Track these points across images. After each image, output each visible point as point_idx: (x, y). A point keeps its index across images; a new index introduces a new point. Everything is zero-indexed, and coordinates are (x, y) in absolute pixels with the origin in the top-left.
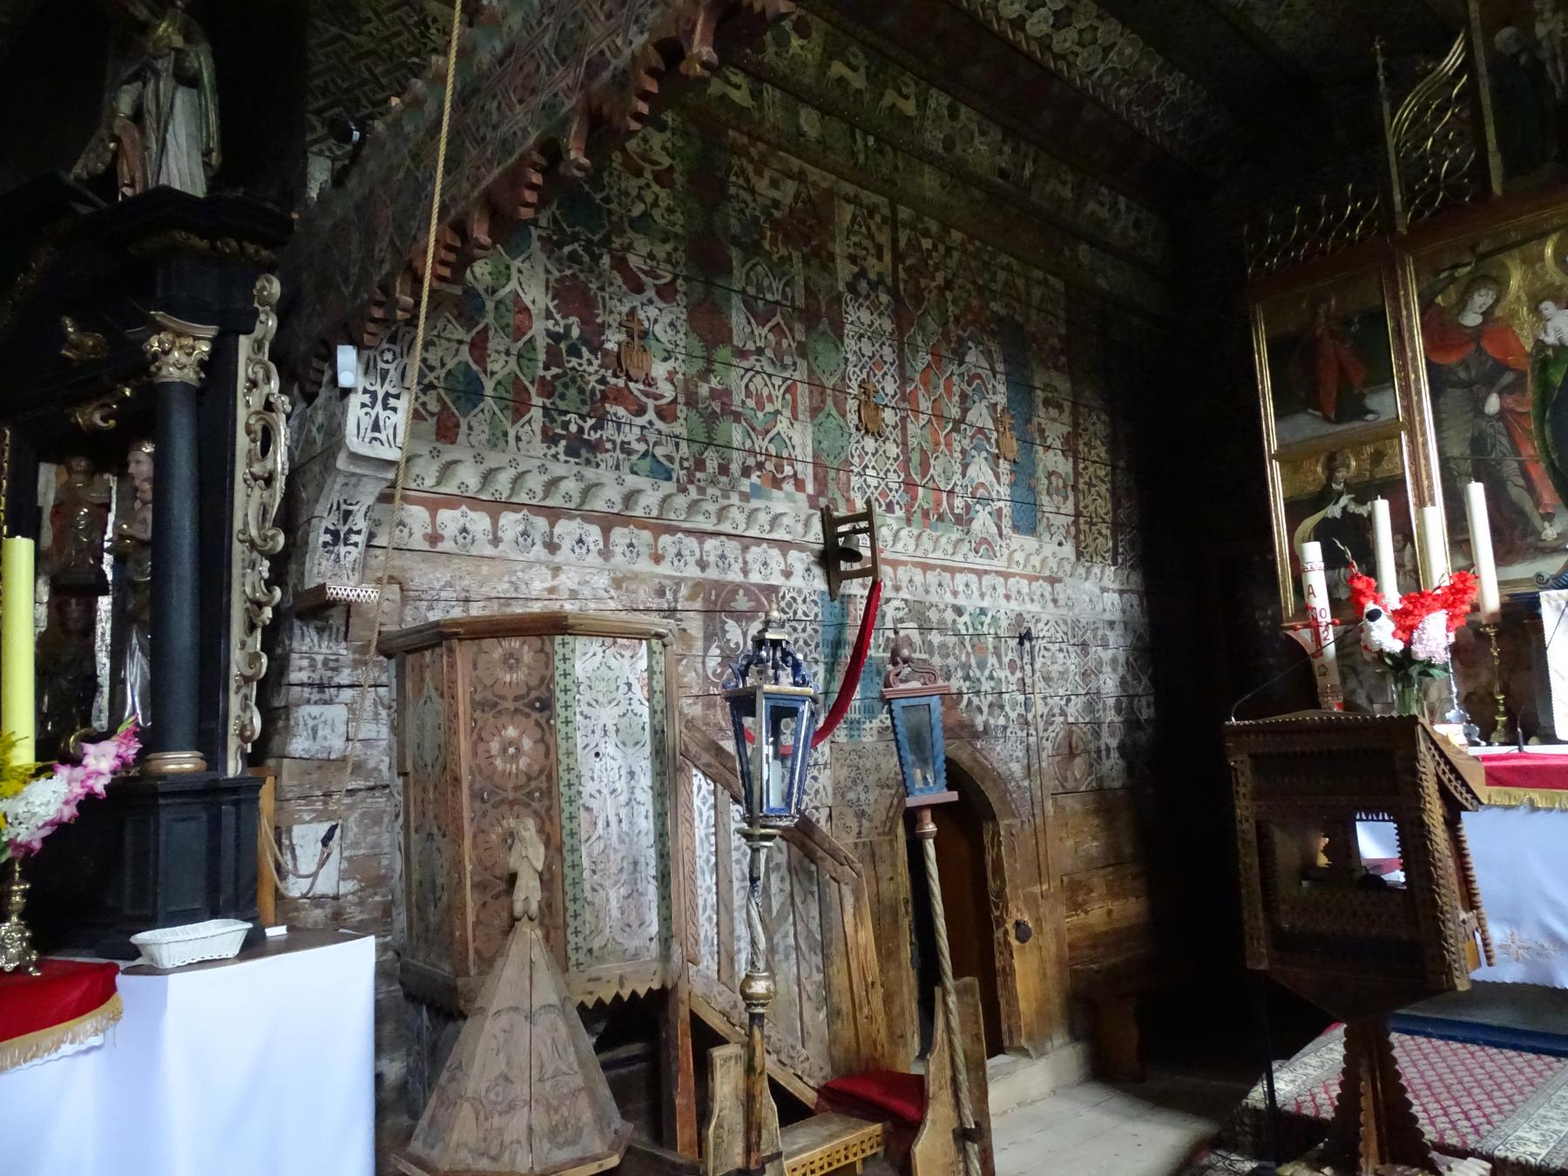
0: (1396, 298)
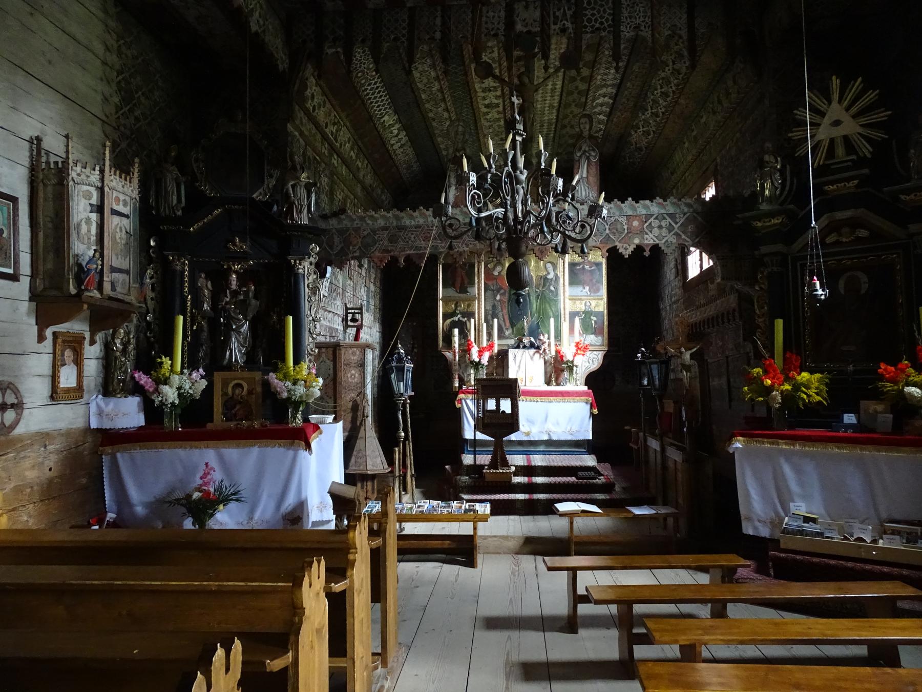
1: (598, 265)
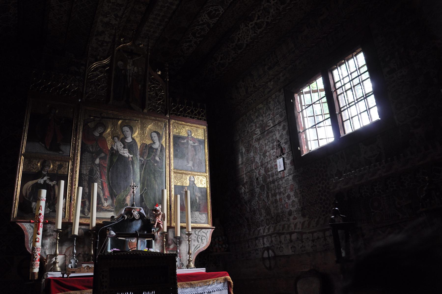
1: (200, 142)
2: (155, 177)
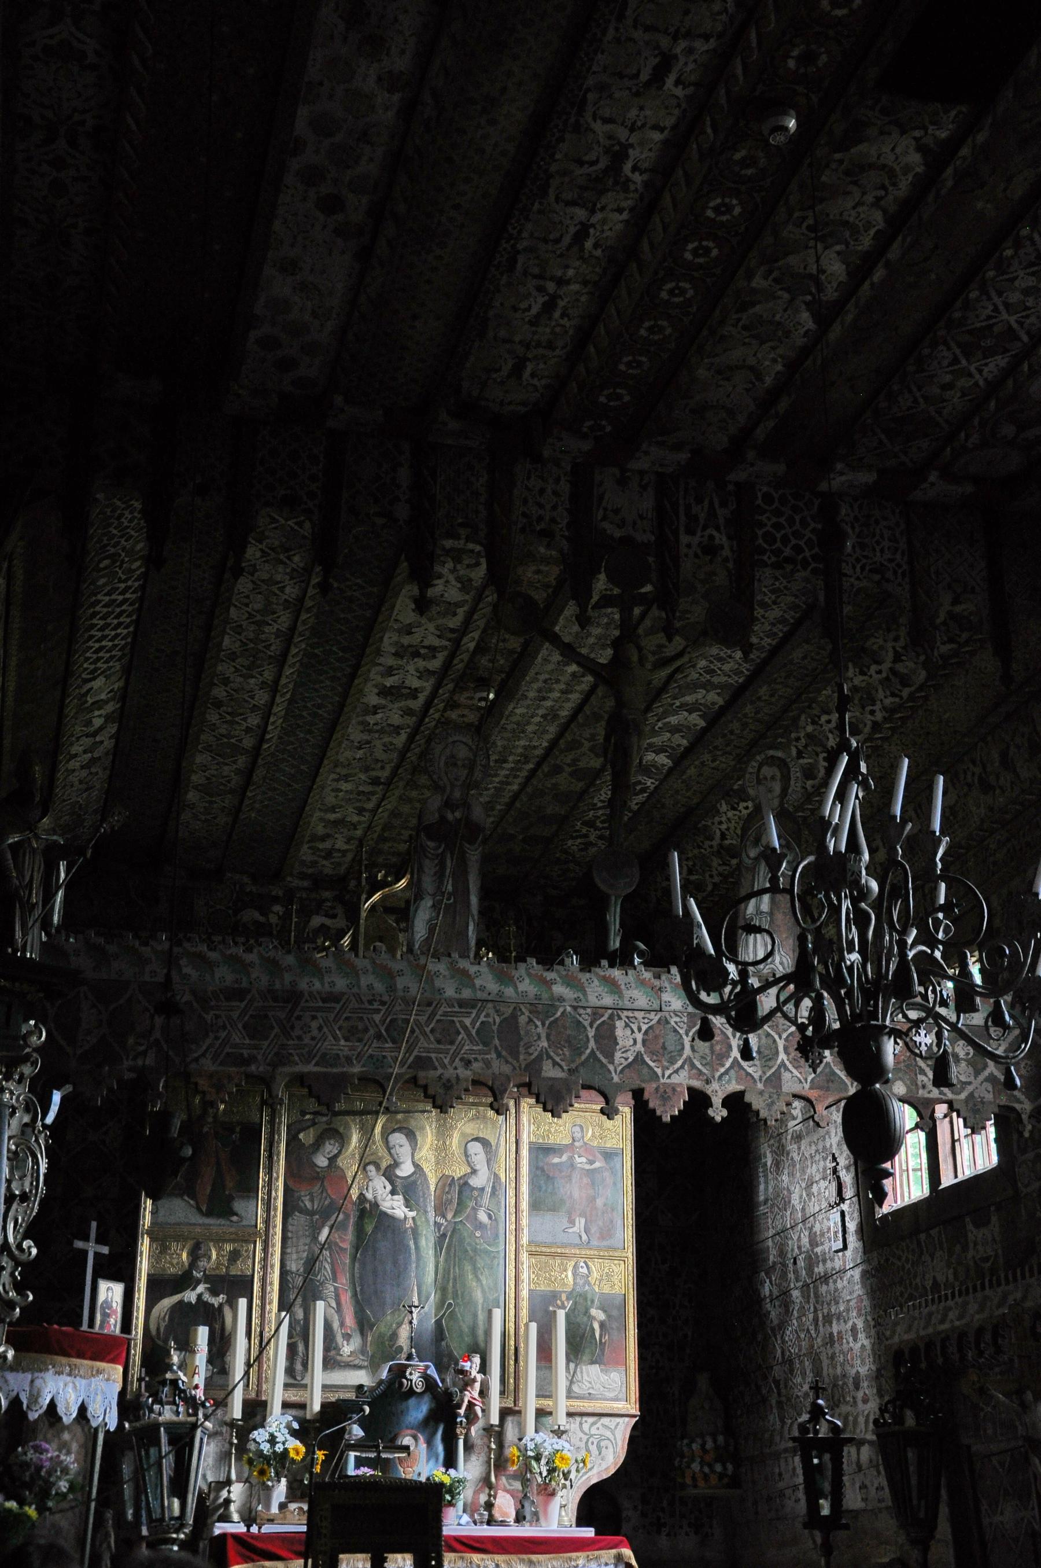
0: (272, 1122)
2: (475, 1270)
